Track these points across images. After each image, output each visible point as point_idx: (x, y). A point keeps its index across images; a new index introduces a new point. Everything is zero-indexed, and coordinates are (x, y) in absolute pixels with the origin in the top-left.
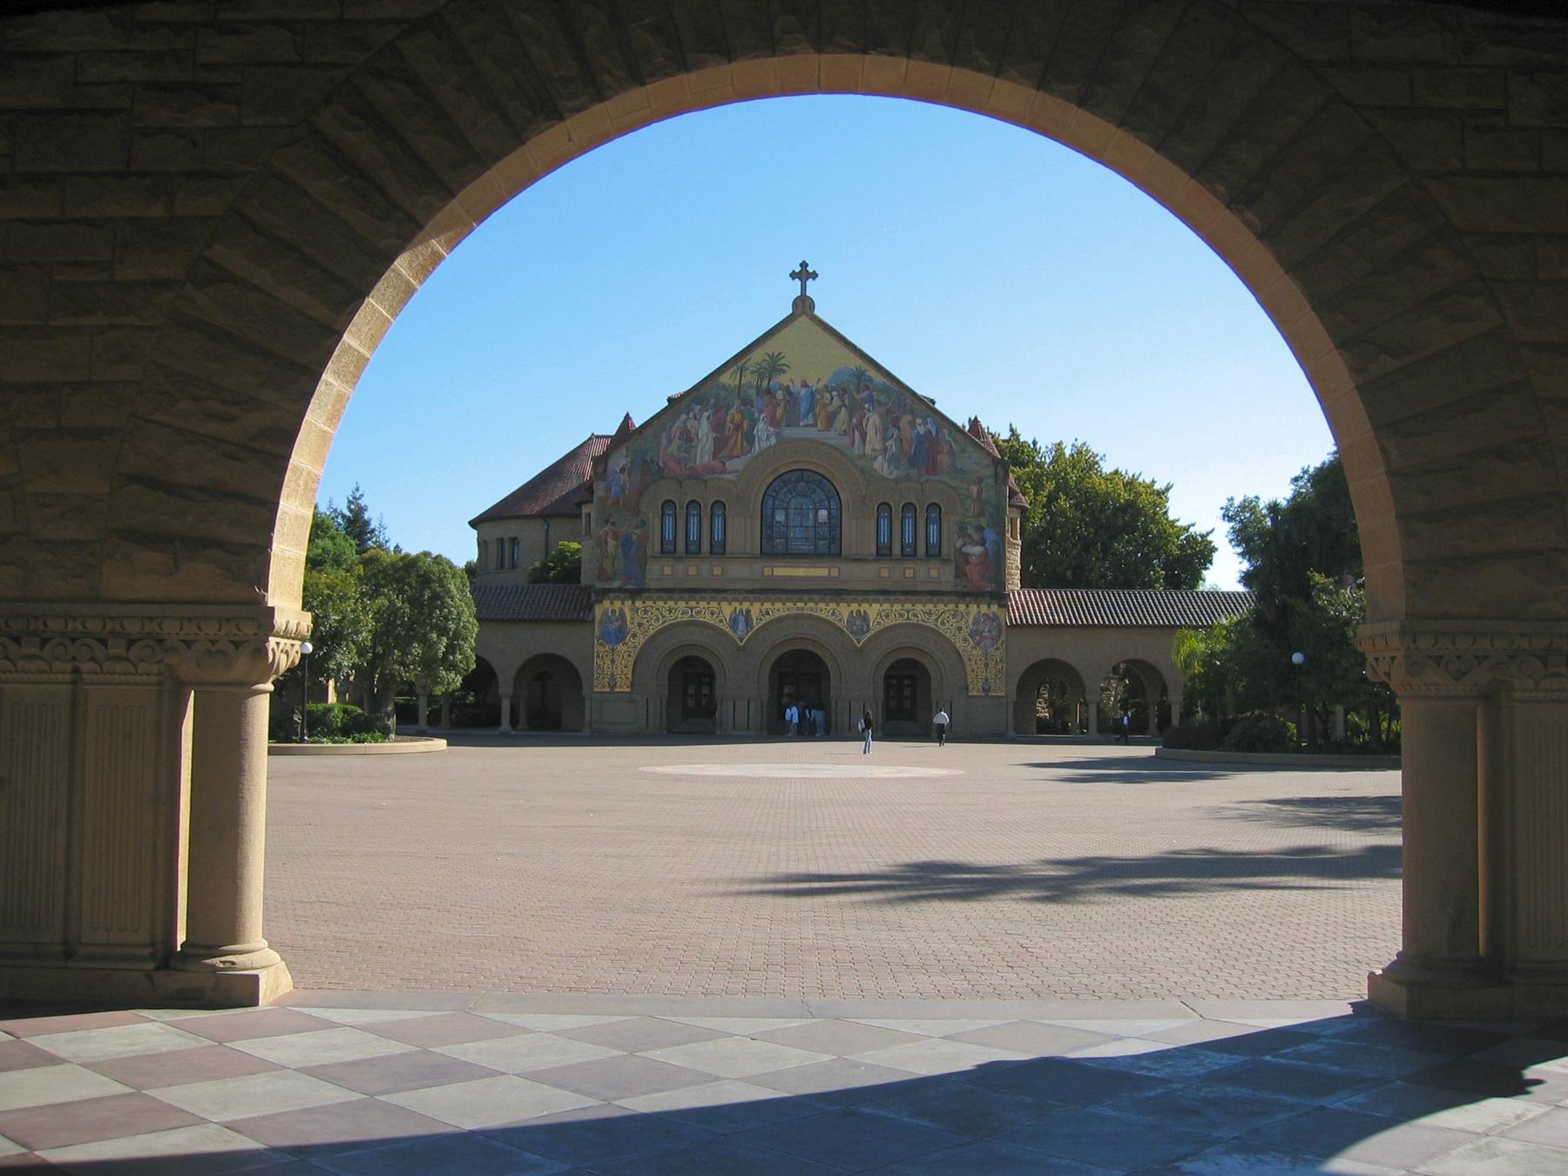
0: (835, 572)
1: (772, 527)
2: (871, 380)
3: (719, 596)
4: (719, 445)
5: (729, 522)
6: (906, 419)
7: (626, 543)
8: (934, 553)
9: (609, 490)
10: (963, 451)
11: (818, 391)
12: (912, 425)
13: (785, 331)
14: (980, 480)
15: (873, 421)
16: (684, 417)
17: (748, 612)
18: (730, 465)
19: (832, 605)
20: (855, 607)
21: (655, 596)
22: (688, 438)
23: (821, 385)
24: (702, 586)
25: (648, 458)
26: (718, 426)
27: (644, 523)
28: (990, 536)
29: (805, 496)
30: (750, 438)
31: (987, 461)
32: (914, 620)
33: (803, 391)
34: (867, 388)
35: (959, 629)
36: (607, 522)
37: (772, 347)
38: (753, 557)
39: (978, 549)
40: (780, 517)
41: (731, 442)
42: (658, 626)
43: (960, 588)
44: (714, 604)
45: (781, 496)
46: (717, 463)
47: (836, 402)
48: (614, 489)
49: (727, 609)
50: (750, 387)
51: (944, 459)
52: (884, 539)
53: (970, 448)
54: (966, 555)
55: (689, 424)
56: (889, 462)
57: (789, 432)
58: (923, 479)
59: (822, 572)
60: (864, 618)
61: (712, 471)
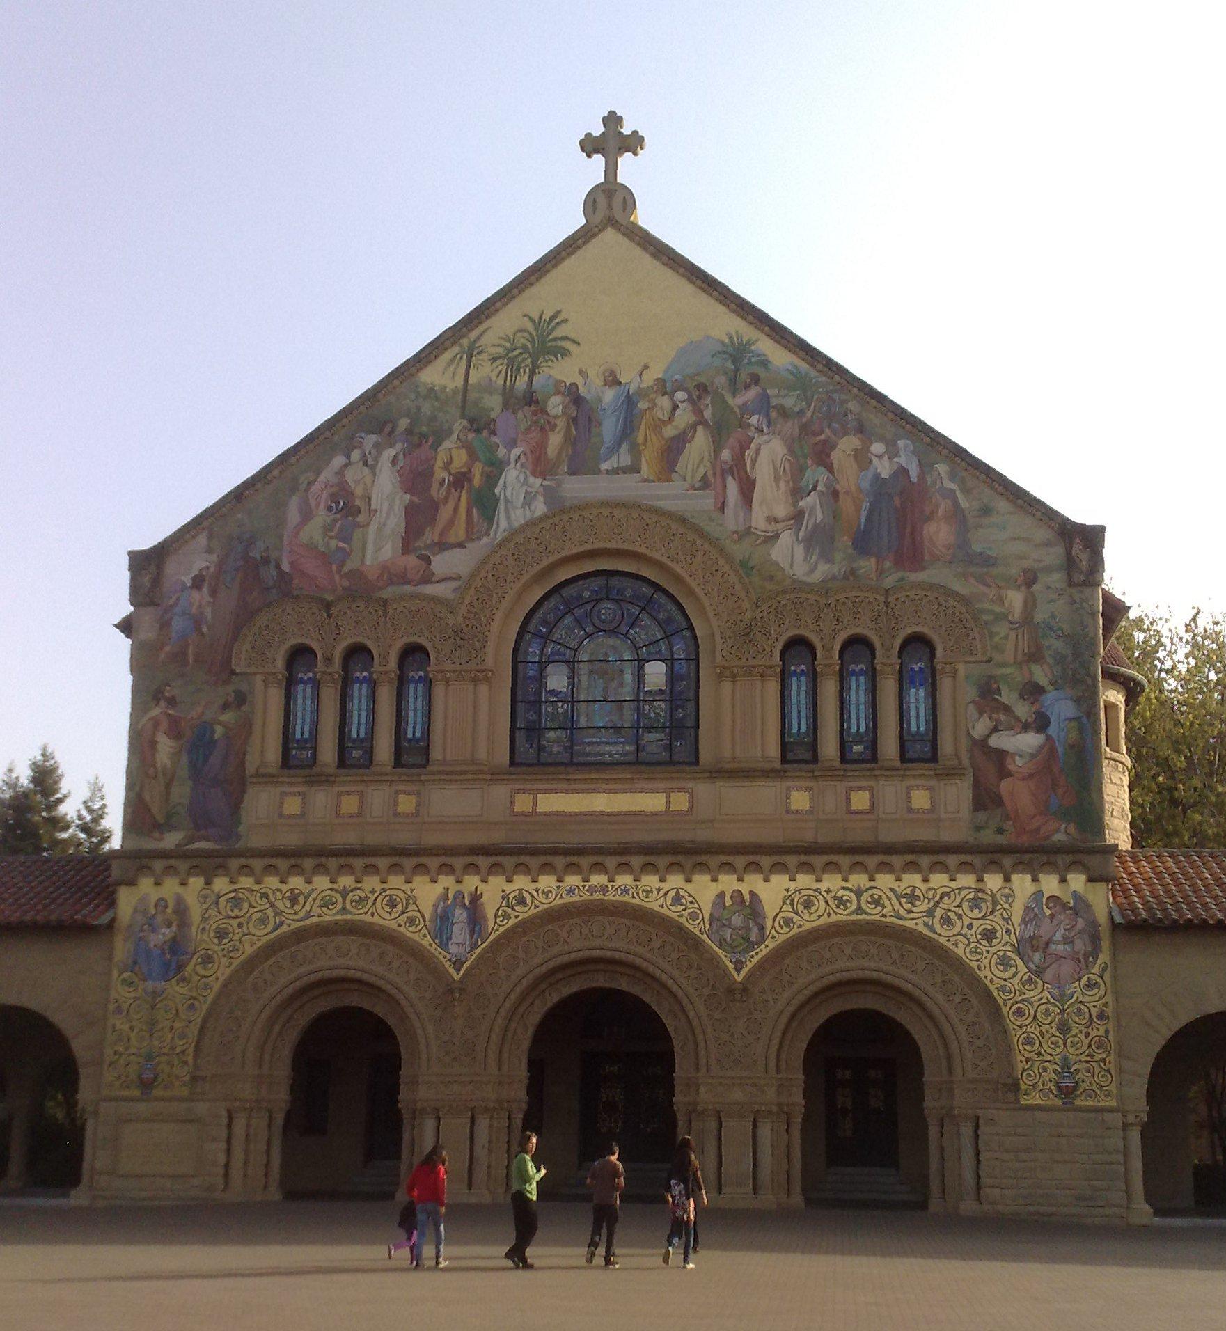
0: (680, 802)
1: (536, 704)
2: (764, 363)
3: (409, 863)
4: (419, 517)
5: (439, 691)
6: (848, 443)
7: (199, 744)
8: (921, 752)
9: (165, 625)
10: (986, 511)
11: (642, 393)
12: (862, 458)
13: (569, 263)
14: (1030, 579)
15: (769, 455)
16: (339, 461)
17: (476, 897)
18: (442, 563)
19: (675, 881)
20: (728, 882)
21: (257, 864)
22: (347, 507)
23: (648, 380)
24: (372, 840)
25: (256, 555)
26: (416, 479)
27: (241, 699)
28: (1061, 708)
29: (614, 632)
30: (486, 504)
31: (1042, 534)
32: (874, 914)
33: (609, 395)
34: (756, 379)
35: (989, 935)
36: (157, 696)
37: (538, 301)
38: (495, 776)
39: (1030, 741)
40: (557, 680)
41: (445, 513)
42: (263, 935)
43: (988, 837)
44: (396, 881)
45: (558, 634)
46: (412, 560)
47: (684, 416)
48: (178, 624)
49: (428, 892)
50: (488, 388)
51: (938, 533)
52: (799, 724)
53: (1003, 505)
54: (1001, 754)
55: (350, 476)
56: (809, 542)
57: (576, 488)
58: (889, 581)
59: (651, 802)
60: (752, 908)
61: (403, 579)
